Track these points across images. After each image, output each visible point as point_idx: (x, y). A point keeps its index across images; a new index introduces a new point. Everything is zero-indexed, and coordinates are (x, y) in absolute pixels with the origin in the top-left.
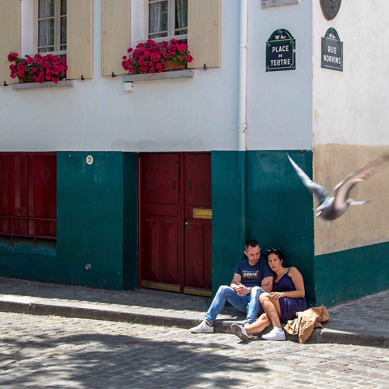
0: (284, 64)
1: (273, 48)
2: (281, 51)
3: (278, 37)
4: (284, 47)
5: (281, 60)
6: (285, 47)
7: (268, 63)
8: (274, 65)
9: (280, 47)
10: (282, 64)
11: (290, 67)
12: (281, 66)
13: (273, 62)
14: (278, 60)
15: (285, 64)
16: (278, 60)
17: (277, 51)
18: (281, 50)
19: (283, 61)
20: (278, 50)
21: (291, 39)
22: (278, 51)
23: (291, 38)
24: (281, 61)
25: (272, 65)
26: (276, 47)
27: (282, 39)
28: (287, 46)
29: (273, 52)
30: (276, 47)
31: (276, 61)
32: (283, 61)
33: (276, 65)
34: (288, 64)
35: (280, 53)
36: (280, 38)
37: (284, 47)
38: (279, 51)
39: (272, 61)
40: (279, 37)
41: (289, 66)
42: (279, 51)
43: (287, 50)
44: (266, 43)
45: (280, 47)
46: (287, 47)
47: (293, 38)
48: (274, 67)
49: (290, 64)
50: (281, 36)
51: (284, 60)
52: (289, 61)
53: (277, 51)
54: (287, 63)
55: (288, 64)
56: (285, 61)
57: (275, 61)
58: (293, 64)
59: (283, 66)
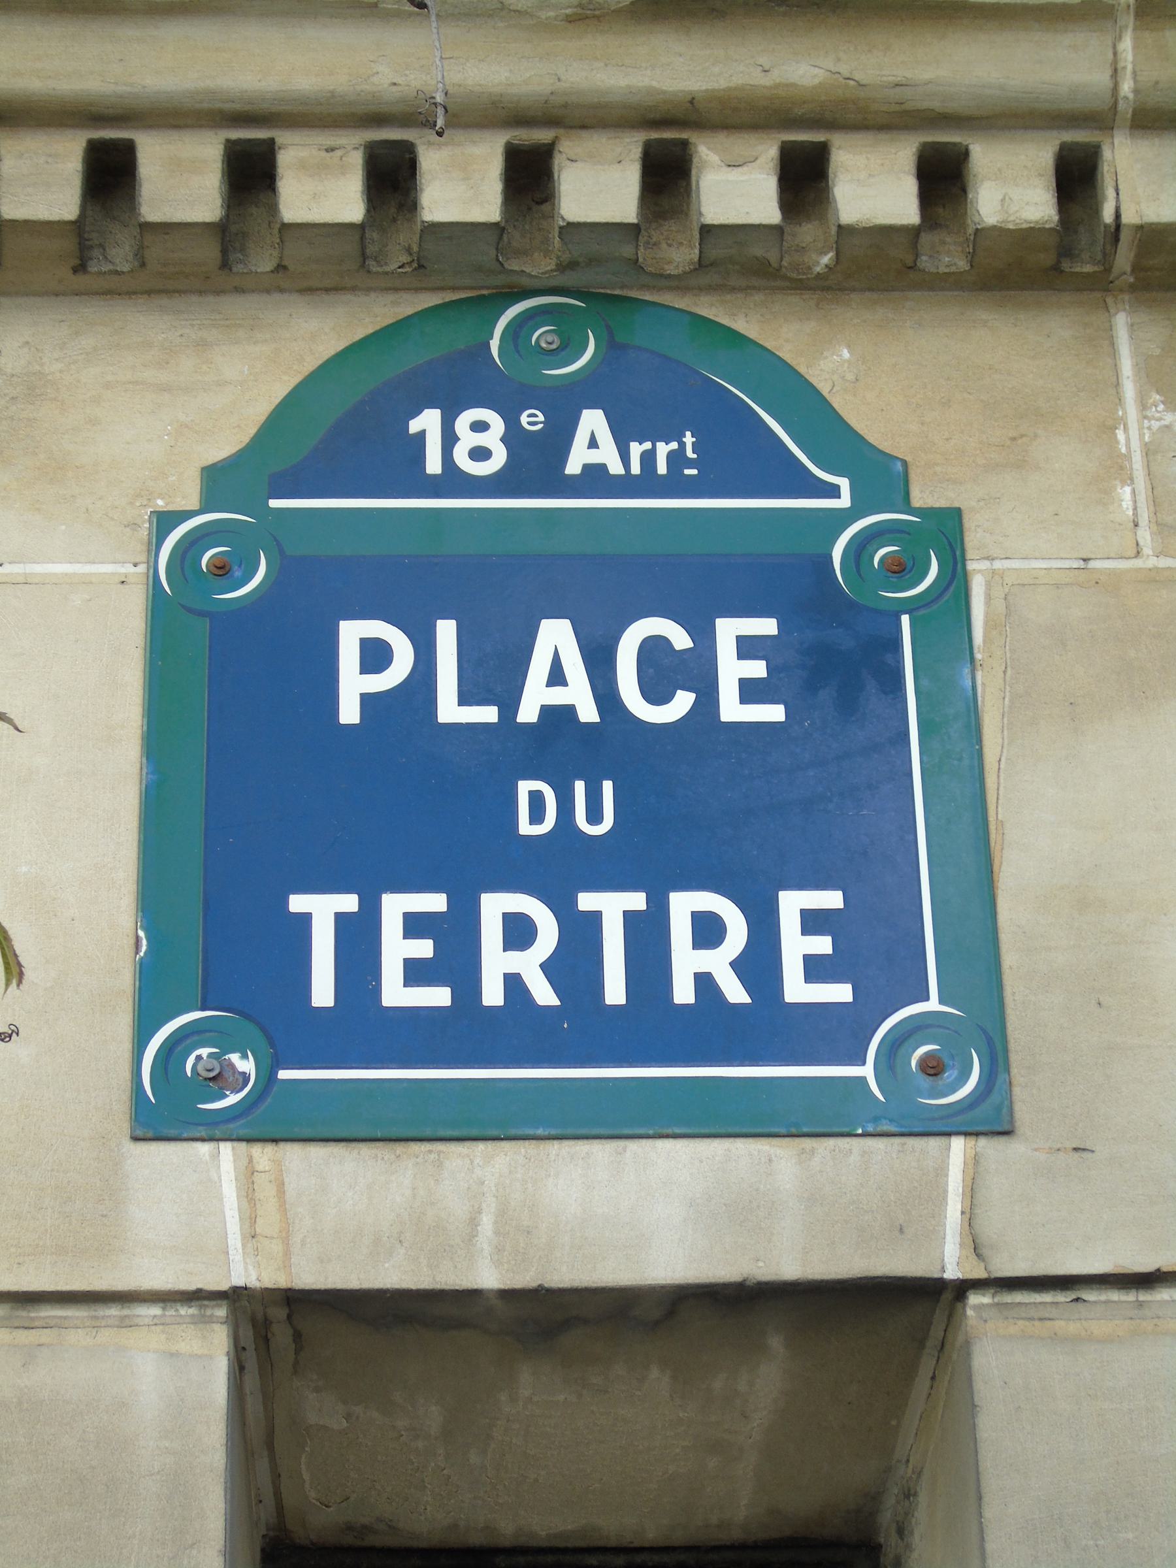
0: (684, 993)
1: (352, 634)
2: (588, 713)
3: (493, 439)
4: (653, 649)
5: (587, 901)
6: (681, 640)
7: (214, 943)
8: (395, 992)
9: (556, 637)
10: (615, 992)
11: (867, 1071)
12: (576, 1024)
13: (358, 940)
14: (494, 906)
15: (704, 982)
16: (494, 906)
17: (450, 710)
18: (580, 697)
19: (646, 935)
21: (834, 492)
22: (488, 714)
23: (844, 483)
24: (595, 918)
25: (323, 993)
26: (446, 632)
27: (595, 480)
28: (728, 630)
29: (349, 713)
30: (446, 632)
31: (436, 902)
32: (646, 935)
33: (439, 996)
34: (797, 989)
36: (536, 463)
37: (653, 649)
38: (528, 713)
39: (323, 910)
40: (513, 436)
41: (833, 1033)
42: (528, 713)
43: (732, 710)
44: (165, 521)
45: (556, 637)
46: (747, 648)
48: (361, 1024)
49: (841, 993)
51: (684, 905)
52: (812, 922)
53: (465, 698)
54: (760, 963)
55: (797, 989)
56: (708, 931)
57: (395, 906)
58: (933, 1004)
59: (655, 1023)
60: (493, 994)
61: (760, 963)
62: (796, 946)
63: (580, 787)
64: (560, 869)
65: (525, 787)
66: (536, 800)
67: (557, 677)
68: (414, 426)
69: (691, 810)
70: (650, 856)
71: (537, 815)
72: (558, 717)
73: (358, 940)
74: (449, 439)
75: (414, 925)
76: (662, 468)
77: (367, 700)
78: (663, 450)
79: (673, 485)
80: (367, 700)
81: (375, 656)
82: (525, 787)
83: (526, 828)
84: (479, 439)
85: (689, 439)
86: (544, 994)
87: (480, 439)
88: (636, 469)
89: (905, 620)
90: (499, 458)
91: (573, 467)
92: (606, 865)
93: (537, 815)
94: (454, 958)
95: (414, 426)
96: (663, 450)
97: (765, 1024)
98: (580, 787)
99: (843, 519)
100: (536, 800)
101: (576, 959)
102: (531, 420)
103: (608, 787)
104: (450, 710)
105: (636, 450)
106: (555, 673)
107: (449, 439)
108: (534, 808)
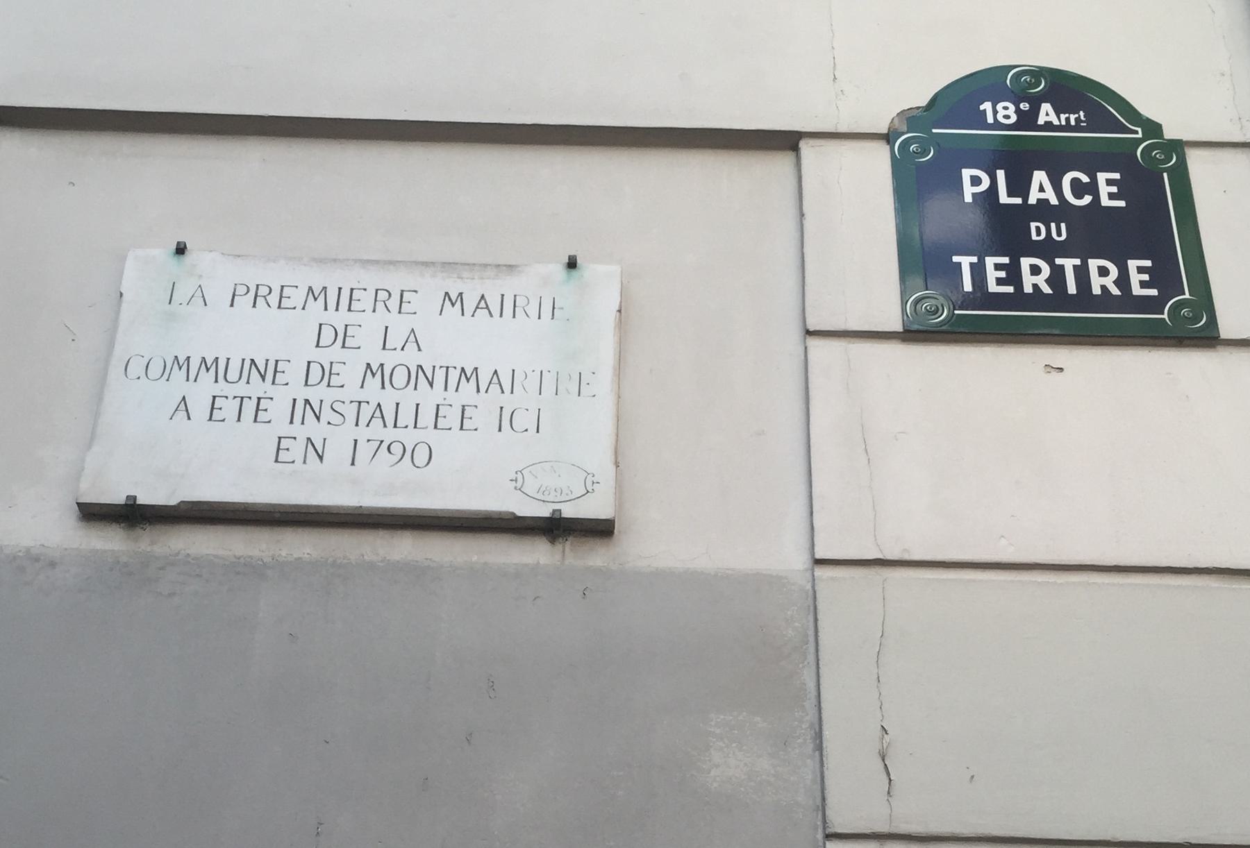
0: (1096, 290)
1: (967, 173)
2: (1054, 201)
4: (1075, 182)
5: (1058, 261)
9: (1040, 177)
10: (1072, 289)
11: (1165, 316)
12: (1059, 298)
13: (978, 272)
14: (1026, 262)
15: (1103, 288)
16: (1026, 262)
17: (1004, 198)
19: (1082, 274)
20: (1019, 185)
21: (1136, 132)
22: (1018, 201)
23: (1139, 130)
27: (1048, 126)
28: (1102, 177)
30: (1001, 174)
31: (1006, 260)
32: (1082, 274)
33: (1010, 289)
34: (1137, 290)
35: (1043, 211)
36: (1027, 120)
37: (1075, 182)
38: (1032, 200)
39: (966, 261)
40: (1018, 111)
42: (1032, 200)
45: (1040, 177)
46: (1110, 182)
47: (1153, 129)
49: (1153, 292)
50: (1035, 111)
51: (1094, 264)
53: (1009, 195)
54: (1123, 281)
58: (1187, 296)
60: (1028, 289)
61: (1123, 281)
62: (1135, 278)
63: (1053, 225)
64: (1048, 250)
65: (1033, 225)
66: (1038, 229)
67: (1042, 189)
68: (982, 107)
69: (1095, 233)
70: (1082, 246)
71: (1039, 233)
72: (1043, 203)
73: (978, 272)
74: (995, 112)
75: (998, 267)
76: (1073, 123)
77: (974, 195)
78: (1073, 117)
79: (1077, 128)
80: (974, 195)
81: (976, 181)
82: (1033, 225)
83: (1034, 237)
84: (1007, 112)
85: (1082, 113)
86: (1047, 290)
87: (1006, 112)
88: (1063, 123)
89: (1165, 175)
90: (1014, 118)
91: (1041, 121)
92: (1065, 250)
93: (1039, 233)
94: (1013, 275)
95: (982, 107)
96: (1073, 117)
97: (1128, 301)
98: (1053, 225)
99: (1140, 141)
100: (1038, 229)
101: (1057, 277)
102: (1024, 106)
103: (1063, 225)
104: (1004, 198)
105: (1063, 117)
106: (1040, 186)
107: (995, 112)
108: (1037, 231)
